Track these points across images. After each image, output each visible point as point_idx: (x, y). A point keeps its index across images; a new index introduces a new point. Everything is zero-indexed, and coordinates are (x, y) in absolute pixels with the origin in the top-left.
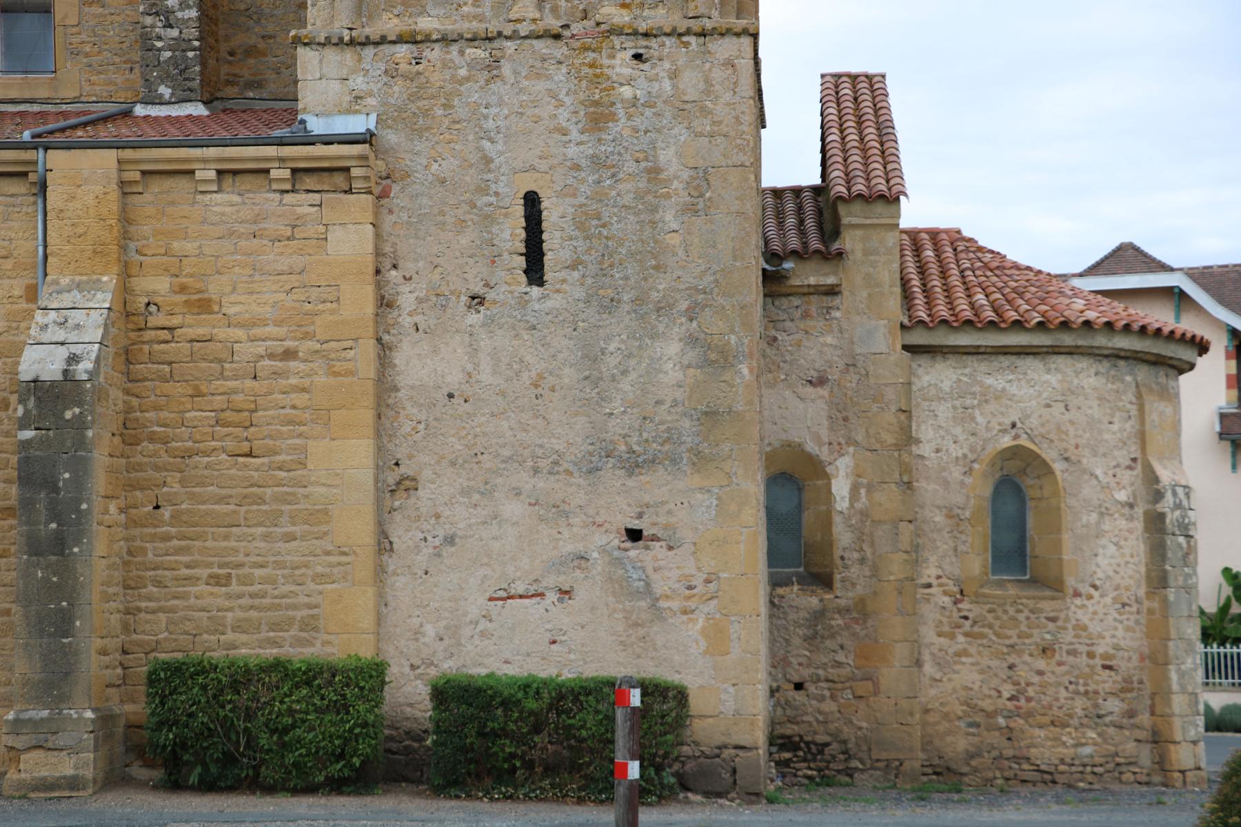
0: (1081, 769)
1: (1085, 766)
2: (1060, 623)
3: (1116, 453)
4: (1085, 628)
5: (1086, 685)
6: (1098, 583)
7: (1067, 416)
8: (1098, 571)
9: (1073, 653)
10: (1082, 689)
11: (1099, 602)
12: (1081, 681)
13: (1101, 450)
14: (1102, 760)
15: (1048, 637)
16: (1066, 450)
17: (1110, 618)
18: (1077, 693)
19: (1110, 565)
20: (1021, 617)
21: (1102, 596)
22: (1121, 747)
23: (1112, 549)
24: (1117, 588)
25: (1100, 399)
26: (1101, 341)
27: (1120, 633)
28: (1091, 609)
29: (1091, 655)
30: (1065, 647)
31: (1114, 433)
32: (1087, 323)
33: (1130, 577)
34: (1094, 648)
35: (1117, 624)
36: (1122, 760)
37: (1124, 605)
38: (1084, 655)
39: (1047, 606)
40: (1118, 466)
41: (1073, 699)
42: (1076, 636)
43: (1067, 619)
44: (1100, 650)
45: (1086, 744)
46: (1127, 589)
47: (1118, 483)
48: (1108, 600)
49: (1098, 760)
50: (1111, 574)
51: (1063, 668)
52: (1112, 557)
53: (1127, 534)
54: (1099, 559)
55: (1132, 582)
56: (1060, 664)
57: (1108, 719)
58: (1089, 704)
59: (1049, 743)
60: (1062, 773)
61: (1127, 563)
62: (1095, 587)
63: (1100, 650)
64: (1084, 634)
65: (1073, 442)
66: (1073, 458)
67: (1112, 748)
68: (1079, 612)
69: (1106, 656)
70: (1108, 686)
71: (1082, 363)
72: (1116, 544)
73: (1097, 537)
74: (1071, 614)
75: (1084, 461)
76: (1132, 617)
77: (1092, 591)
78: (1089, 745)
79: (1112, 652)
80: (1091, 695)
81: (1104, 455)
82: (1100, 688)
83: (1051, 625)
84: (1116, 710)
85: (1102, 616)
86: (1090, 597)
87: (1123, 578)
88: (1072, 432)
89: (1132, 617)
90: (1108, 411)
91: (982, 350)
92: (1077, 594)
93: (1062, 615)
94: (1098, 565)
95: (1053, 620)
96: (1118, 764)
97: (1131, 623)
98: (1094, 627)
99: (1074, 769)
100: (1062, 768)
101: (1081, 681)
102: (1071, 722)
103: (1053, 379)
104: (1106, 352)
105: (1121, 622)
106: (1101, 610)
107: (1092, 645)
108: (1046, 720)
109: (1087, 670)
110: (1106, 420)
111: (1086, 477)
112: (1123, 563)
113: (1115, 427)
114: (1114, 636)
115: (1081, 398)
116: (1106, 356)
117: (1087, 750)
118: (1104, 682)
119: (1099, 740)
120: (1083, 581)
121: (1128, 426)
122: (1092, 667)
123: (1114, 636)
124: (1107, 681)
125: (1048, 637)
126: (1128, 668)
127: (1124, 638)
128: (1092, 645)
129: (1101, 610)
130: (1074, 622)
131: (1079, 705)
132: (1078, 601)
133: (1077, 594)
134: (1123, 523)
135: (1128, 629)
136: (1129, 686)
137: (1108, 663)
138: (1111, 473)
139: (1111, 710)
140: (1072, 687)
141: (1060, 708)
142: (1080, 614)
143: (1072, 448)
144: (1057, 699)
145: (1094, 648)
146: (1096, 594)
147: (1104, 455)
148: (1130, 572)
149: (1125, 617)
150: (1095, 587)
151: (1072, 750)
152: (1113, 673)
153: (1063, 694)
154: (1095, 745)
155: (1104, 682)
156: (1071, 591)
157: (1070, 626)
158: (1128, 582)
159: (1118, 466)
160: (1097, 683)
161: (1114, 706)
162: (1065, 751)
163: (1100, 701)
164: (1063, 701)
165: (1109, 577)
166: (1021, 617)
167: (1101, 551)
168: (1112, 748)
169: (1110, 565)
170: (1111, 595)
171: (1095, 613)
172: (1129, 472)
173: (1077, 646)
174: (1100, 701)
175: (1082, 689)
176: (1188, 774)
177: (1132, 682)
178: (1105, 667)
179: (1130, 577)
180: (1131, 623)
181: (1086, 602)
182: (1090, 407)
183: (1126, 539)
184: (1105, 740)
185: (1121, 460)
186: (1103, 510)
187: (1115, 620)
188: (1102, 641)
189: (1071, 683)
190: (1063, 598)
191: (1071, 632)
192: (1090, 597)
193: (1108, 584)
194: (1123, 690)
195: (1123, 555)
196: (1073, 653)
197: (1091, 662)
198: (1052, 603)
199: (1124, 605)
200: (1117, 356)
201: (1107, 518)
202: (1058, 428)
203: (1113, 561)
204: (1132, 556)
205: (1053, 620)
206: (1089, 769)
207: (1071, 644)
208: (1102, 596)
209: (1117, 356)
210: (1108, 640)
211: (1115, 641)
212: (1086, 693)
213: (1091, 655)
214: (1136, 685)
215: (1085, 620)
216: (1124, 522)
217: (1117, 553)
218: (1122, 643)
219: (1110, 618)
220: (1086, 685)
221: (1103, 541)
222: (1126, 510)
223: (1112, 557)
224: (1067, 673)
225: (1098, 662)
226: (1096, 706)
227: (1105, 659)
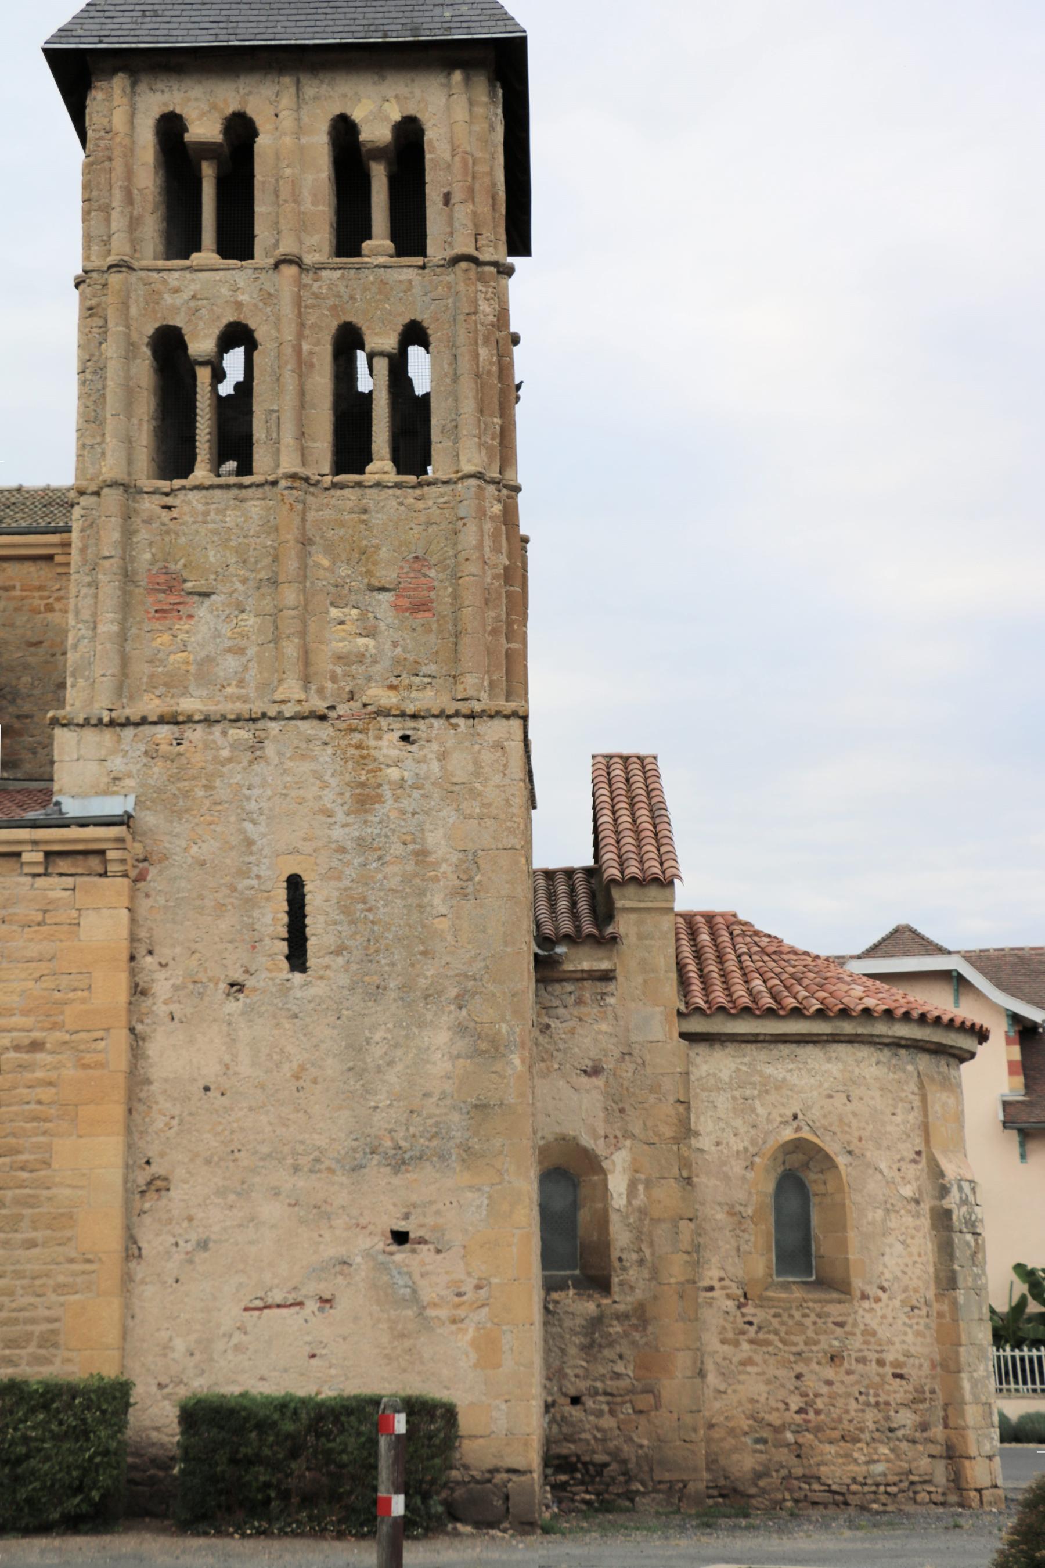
0: (874, 1488)
1: (878, 1485)
2: (848, 1328)
3: (900, 1146)
4: (874, 1334)
5: (876, 1395)
6: (886, 1284)
7: (850, 1107)
8: (886, 1271)
9: (862, 1360)
10: (872, 1400)
11: (887, 1306)
12: (872, 1391)
13: (885, 1143)
14: (896, 1479)
15: (836, 1343)
16: (849, 1143)
17: (900, 1322)
18: (868, 1404)
19: (898, 1264)
20: (808, 1322)
21: (890, 1298)
23: (899, 1247)
24: (905, 1290)
25: (881, 1089)
26: (881, 1029)
27: (910, 1338)
28: (879, 1313)
29: (881, 1363)
30: (854, 1355)
31: (897, 1125)
32: (867, 1011)
33: (919, 1278)
34: (884, 1355)
36: (916, 1478)
38: (874, 1363)
39: (835, 1310)
40: (902, 1159)
41: (863, 1411)
42: (866, 1342)
43: (855, 1324)
44: (889, 1357)
45: (878, 1461)
47: (903, 1178)
48: (897, 1303)
50: (899, 1274)
51: (852, 1378)
52: (899, 1256)
54: (886, 1258)
55: (920, 1284)
56: (849, 1373)
57: (900, 1433)
58: (880, 1416)
59: (840, 1461)
60: (854, 1493)
61: (915, 1262)
62: (883, 1289)
63: (889, 1357)
64: (872, 1340)
65: (856, 1134)
66: (857, 1151)
67: (906, 1466)
68: (868, 1316)
69: (896, 1364)
70: (899, 1397)
71: (864, 1052)
74: (859, 1319)
75: (868, 1154)
76: (922, 1321)
77: (880, 1293)
78: (878, 1462)
79: (902, 1359)
80: (882, 1406)
81: (889, 1148)
82: (891, 1399)
83: (839, 1330)
84: (909, 1423)
85: (890, 1320)
86: (878, 1300)
90: (890, 1102)
91: (761, 1038)
92: (864, 1297)
93: (850, 1320)
94: (885, 1266)
95: (841, 1325)
96: (912, 1483)
97: (921, 1328)
98: (883, 1333)
99: (866, 1489)
101: (872, 1391)
102: (862, 1436)
103: (834, 1068)
104: (887, 1041)
105: (911, 1326)
106: (890, 1314)
107: (882, 1351)
108: (836, 1434)
109: (877, 1379)
110: (888, 1111)
111: (870, 1171)
112: (910, 1263)
113: (898, 1119)
114: (903, 1342)
116: (887, 1045)
117: (879, 1468)
118: (895, 1392)
119: (892, 1456)
120: (870, 1283)
124: (898, 1391)
125: (836, 1343)
126: (920, 1377)
127: (914, 1344)
128: (882, 1351)
129: (890, 1314)
130: (862, 1327)
131: (870, 1417)
132: (866, 1304)
133: (864, 1297)
134: (909, 1220)
137: (898, 1371)
138: (895, 1167)
139: (903, 1422)
140: (862, 1398)
141: (851, 1421)
143: (856, 1141)
144: (847, 1412)
146: (884, 1296)
148: (918, 1272)
149: (914, 1321)
150: (883, 1289)
151: (864, 1468)
152: (904, 1382)
153: (853, 1405)
154: (888, 1461)
156: (858, 1294)
157: (858, 1331)
159: (902, 1159)
160: (888, 1393)
161: (906, 1418)
162: (857, 1469)
163: (892, 1413)
164: (853, 1413)
165: (896, 1278)
166: (808, 1322)
167: (887, 1250)
168: (906, 1466)
169: (898, 1264)
170: (899, 1298)
171: (884, 1317)
173: (866, 1353)
174: (892, 1413)
175: (872, 1400)
176: (984, 1492)
177: (924, 1392)
178: (896, 1376)
179: (919, 1278)
180: (921, 1328)
181: (874, 1305)
182: (873, 1098)
183: (913, 1238)
184: (898, 1456)
185: (905, 1154)
186: (889, 1206)
187: (904, 1324)
189: (861, 1393)
190: (851, 1301)
191: (860, 1338)
192: (878, 1300)
193: (896, 1285)
194: (914, 1401)
195: (910, 1255)
196: (862, 1360)
197: (881, 1370)
198: (839, 1306)
199: (913, 1308)
200: (897, 1044)
201: (893, 1215)
202: (841, 1120)
203: (900, 1261)
204: (920, 1255)
206: (882, 1489)
207: (860, 1350)
208: (890, 1298)
209: (897, 1044)
210: (898, 1346)
211: (905, 1347)
212: (877, 1404)
213: (881, 1363)
214: (928, 1395)
215: (874, 1324)
216: (910, 1219)
218: (913, 1350)
219: (900, 1322)
220: (876, 1395)
221: (890, 1239)
222: (913, 1206)
224: (857, 1382)
225: (888, 1370)
226: (888, 1418)
227: (896, 1367)
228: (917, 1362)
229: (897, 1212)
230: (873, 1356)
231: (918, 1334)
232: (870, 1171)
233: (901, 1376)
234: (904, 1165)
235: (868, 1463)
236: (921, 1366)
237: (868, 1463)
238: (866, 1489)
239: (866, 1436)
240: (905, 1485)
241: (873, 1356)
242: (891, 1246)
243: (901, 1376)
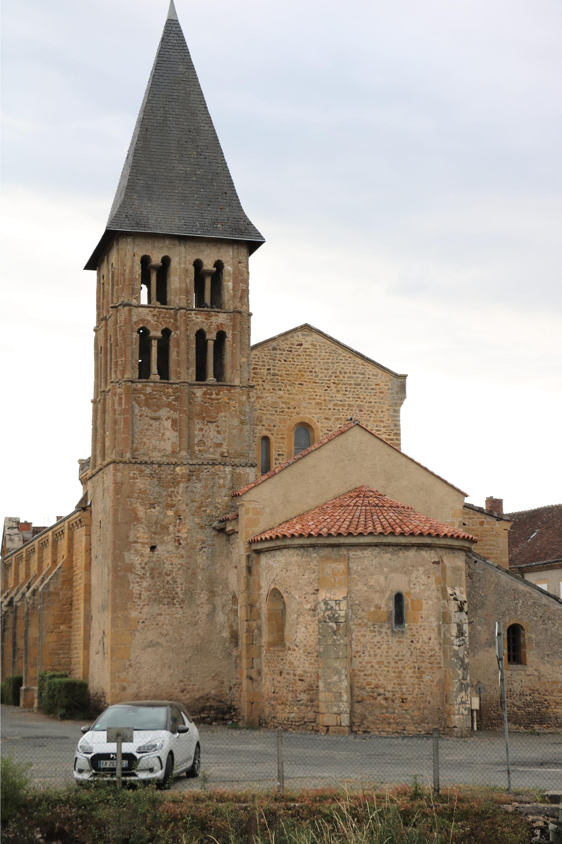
1: (292, 722)
2: (284, 661)
3: (306, 588)
4: (292, 663)
5: (292, 687)
6: (298, 644)
9: (288, 674)
10: (291, 689)
13: (298, 587)
14: (298, 720)
15: (281, 667)
16: (286, 588)
17: (302, 659)
18: (289, 690)
19: (302, 636)
21: (299, 650)
22: (306, 715)
24: (305, 646)
25: (298, 566)
26: (288, 542)
27: (307, 665)
28: (295, 655)
29: (295, 675)
31: (305, 580)
32: (293, 536)
33: (313, 641)
34: (296, 672)
35: (306, 662)
37: (309, 653)
40: (307, 593)
42: (290, 667)
43: (286, 660)
44: (298, 672)
45: (292, 713)
46: (310, 646)
47: (307, 601)
48: (301, 651)
49: (297, 719)
50: (303, 640)
51: (285, 680)
52: (303, 633)
53: (311, 622)
54: (298, 634)
55: (313, 643)
56: (284, 678)
57: (301, 702)
58: (294, 695)
60: (285, 724)
61: (311, 635)
62: (297, 646)
63: (298, 672)
64: (292, 666)
65: (288, 585)
67: (303, 715)
68: (291, 657)
70: (302, 688)
71: (292, 551)
72: (305, 627)
73: (297, 624)
75: (292, 592)
76: (313, 659)
77: (295, 647)
79: (302, 673)
81: (300, 589)
83: (282, 662)
84: (304, 698)
85: (298, 658)
86: (294, 650)
87: (308, 642)
88: (288, 581)
89: (313, 659)
90: (302, 570)
91: (271, 549)
92: (289, 649)
93: (285, 658)
94: (297, 636)
95: (282, 660)
96: (306, 722)
97: (312, 661)
98: (296, 663)
99: (288, 723)
100: (285, 722)
102: (288, 703)
103: (282, 559)
105: (307, 661)
106: (298, 655)
107: (295, 670)
108: (280, 702)
109: (293, 681)
110: (301, 575)
111: (293, 599)
112: (308, 635)
113: (306, 577)
114: (303, 667)
115: (292, 566)
116: (296, 548)
117: (293, 715)
118: (300, 686)
119: (298, 711)
120: (291, 643)
121: (313, 576)
122: (295, 680)
123: (303, 667)
124: (301, 686)
126: (310, 681)
129: (298, 655)
130: (288, 661)
131: (290, 695)
132: (290, 652)
133: (289, 649)
135: (311, 664)
136: (311, 688)
137: (301, 678)
138: (303, 597)
139: (302, 698)
140: (288, 688)
142: (291, 658)
145: (296, 672)
146: (297, 649)
147: (300, 589)
148: (313, 639)
149: (309, 658)
150: (297, 646)
151: (288, 715)
152: (303, 683)
153: (285, 691)
154: (296, 713)
155: (300, 686)
156: (287, 648)
157: (287, 662)
158: (311, 643)
159: (307, 593)
160: (297, 686)
161: (304, 697)
162: (286, 715)
163: (298, 694)
165: (301, 641)
166: (275, 658)
167: (298, 630)
169: (302, 636)
171: (296, 657)
172: (313, 596)
174: (298, 694)
175: (291, 689)
176: (330, 728)
177: (313, 687)
178: (300, 680)
179: (313, 641)
180: (312, 661)
181: (293, 652)
182: (295, 570)
183: (310, 625)
184: (300, 711)
185: (308, 591)
187: (304, 660)
188: (298, 669)
190: (285, 651)
191: (288, 664)
192: (294, 650)
194: (308, 690)
195: (308, 632)
196: (288, 674)
197: (294, 678)
199: (309, 653)
200: (302, 547)
201: (301, 617)
202: (284, 580)
203: (303, 635)
204: (314, 632)
205: (282, 660)
206: (294, 723)
208: (299, 650)
209: (302, 547)
210: (301, 668)
211: (304, 669)
212: (293, 691)
213: (295, 675)
214: (314, 688)
215: (292, 660)
216: (309, 618)
217: (306, 631)
218: (307, 670)
219: (302, 659)
221: (299, 626)
222: (311, 612)
223: (303, 633)
224: (286, 682)
225: (297, 678)
226: (296, 697)
228: (309, 675)
229: (303, 615)
230: (292, 672)
231: (311, 664)
232: (293, 599)
233: (302, 680)
234: (307, 596)
235: (289, 713)
236: (311, 676)
237: (289, 713)
238: (288, 723)
239: (289, 703)
240: (302, 722)
241: (292, 672)
242: (300, 629)
243: (302, 680)
